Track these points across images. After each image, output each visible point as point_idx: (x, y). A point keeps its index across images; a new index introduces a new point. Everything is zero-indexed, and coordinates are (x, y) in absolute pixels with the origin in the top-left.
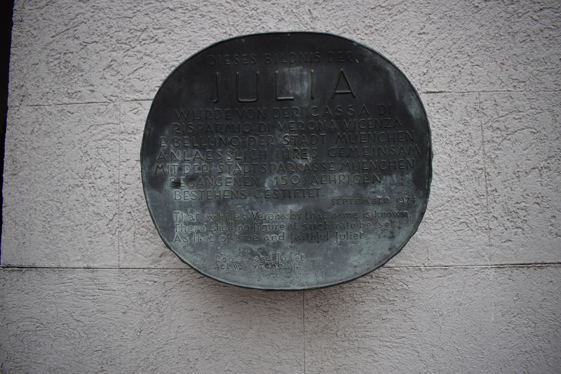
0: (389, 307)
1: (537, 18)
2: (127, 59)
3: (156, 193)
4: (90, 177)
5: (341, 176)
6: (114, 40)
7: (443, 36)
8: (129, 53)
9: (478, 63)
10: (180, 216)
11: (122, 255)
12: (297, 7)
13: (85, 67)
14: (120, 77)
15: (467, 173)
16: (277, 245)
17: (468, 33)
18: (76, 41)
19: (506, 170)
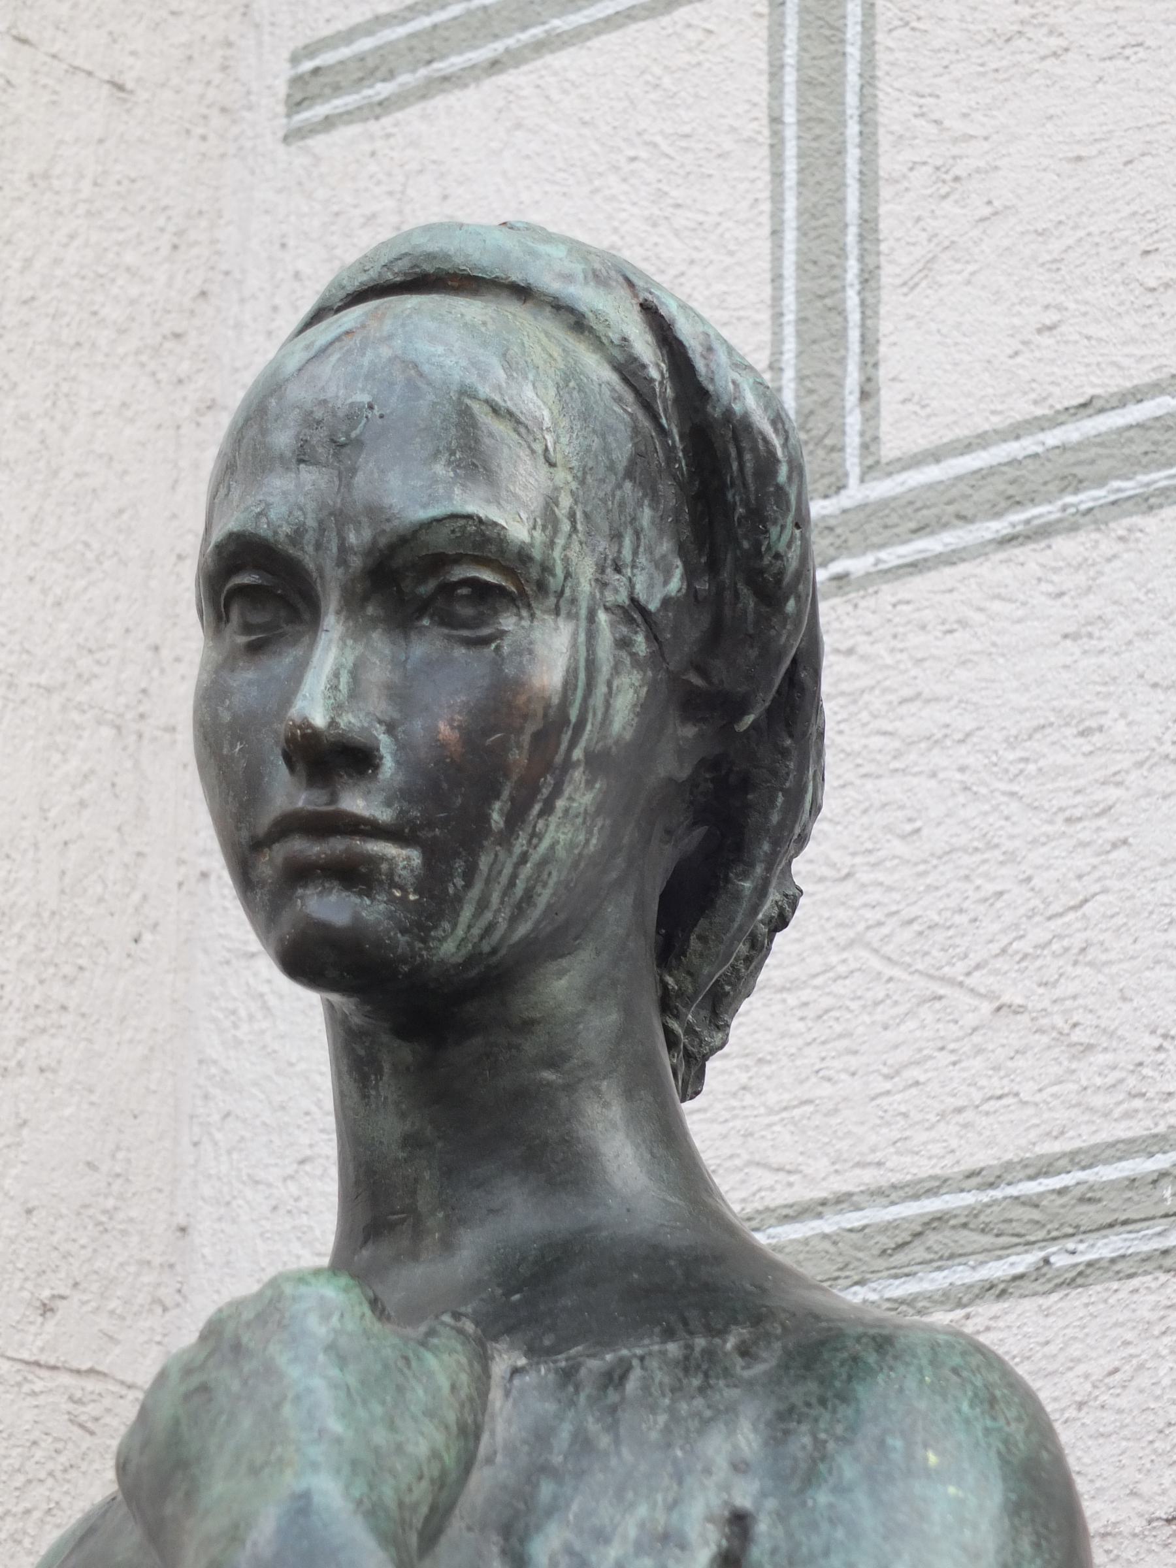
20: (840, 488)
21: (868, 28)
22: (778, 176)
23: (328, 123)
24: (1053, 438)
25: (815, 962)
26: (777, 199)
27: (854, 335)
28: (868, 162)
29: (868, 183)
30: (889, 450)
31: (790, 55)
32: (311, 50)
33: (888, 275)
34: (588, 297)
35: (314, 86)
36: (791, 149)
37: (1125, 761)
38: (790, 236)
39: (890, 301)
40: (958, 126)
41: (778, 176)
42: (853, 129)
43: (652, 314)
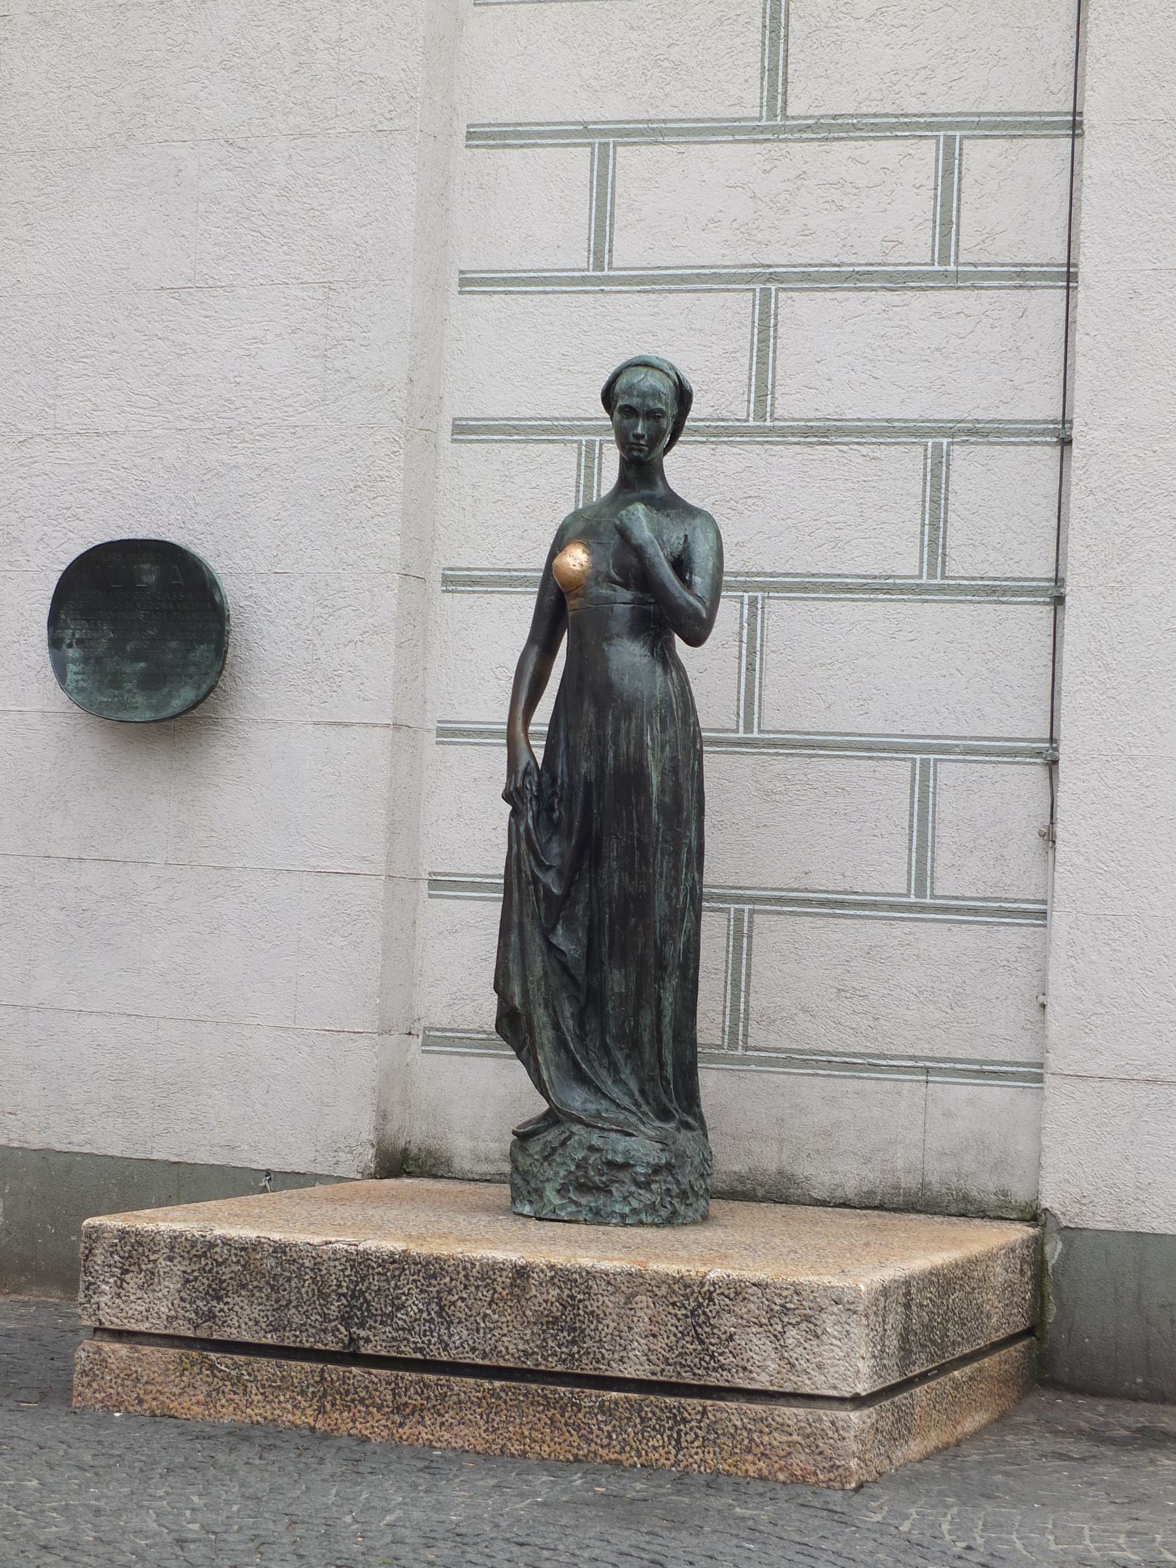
0: (232, 751)
1: (370, 506)
2: (55, 534)
3: (55, 650)
4: (24, 635)
5: (174, 645)
6: (45, 516)
7: (293, 522)
8: (57, 528)
9: (318, 547)
10: (72, 668)
11: (46, 701)
12: (185, 493)
13: (23, 538)
14: (50, 550)
15: (300, 643)
16: (129, 691)
17: (313, 520)
18: (16, 515)
19: (329, 642)
20: (603, 270)
21: (614, 168)
22: (591, 196)
23: (477, 146)
24: (651, 272)
25: (593, 370)
26: (591, 201)
27: (608, 237)
28: (613, 199)
31: (596, 167)
32: (473, 126)
33: (616, 226)
34: (670, 372)
35: (473, 135)
36: (595, 190)
37: (661, 343)
38: (594, 210)
40: (635, 198)
41: (591, 196)
42: (609, 190)
43: (678, 376)
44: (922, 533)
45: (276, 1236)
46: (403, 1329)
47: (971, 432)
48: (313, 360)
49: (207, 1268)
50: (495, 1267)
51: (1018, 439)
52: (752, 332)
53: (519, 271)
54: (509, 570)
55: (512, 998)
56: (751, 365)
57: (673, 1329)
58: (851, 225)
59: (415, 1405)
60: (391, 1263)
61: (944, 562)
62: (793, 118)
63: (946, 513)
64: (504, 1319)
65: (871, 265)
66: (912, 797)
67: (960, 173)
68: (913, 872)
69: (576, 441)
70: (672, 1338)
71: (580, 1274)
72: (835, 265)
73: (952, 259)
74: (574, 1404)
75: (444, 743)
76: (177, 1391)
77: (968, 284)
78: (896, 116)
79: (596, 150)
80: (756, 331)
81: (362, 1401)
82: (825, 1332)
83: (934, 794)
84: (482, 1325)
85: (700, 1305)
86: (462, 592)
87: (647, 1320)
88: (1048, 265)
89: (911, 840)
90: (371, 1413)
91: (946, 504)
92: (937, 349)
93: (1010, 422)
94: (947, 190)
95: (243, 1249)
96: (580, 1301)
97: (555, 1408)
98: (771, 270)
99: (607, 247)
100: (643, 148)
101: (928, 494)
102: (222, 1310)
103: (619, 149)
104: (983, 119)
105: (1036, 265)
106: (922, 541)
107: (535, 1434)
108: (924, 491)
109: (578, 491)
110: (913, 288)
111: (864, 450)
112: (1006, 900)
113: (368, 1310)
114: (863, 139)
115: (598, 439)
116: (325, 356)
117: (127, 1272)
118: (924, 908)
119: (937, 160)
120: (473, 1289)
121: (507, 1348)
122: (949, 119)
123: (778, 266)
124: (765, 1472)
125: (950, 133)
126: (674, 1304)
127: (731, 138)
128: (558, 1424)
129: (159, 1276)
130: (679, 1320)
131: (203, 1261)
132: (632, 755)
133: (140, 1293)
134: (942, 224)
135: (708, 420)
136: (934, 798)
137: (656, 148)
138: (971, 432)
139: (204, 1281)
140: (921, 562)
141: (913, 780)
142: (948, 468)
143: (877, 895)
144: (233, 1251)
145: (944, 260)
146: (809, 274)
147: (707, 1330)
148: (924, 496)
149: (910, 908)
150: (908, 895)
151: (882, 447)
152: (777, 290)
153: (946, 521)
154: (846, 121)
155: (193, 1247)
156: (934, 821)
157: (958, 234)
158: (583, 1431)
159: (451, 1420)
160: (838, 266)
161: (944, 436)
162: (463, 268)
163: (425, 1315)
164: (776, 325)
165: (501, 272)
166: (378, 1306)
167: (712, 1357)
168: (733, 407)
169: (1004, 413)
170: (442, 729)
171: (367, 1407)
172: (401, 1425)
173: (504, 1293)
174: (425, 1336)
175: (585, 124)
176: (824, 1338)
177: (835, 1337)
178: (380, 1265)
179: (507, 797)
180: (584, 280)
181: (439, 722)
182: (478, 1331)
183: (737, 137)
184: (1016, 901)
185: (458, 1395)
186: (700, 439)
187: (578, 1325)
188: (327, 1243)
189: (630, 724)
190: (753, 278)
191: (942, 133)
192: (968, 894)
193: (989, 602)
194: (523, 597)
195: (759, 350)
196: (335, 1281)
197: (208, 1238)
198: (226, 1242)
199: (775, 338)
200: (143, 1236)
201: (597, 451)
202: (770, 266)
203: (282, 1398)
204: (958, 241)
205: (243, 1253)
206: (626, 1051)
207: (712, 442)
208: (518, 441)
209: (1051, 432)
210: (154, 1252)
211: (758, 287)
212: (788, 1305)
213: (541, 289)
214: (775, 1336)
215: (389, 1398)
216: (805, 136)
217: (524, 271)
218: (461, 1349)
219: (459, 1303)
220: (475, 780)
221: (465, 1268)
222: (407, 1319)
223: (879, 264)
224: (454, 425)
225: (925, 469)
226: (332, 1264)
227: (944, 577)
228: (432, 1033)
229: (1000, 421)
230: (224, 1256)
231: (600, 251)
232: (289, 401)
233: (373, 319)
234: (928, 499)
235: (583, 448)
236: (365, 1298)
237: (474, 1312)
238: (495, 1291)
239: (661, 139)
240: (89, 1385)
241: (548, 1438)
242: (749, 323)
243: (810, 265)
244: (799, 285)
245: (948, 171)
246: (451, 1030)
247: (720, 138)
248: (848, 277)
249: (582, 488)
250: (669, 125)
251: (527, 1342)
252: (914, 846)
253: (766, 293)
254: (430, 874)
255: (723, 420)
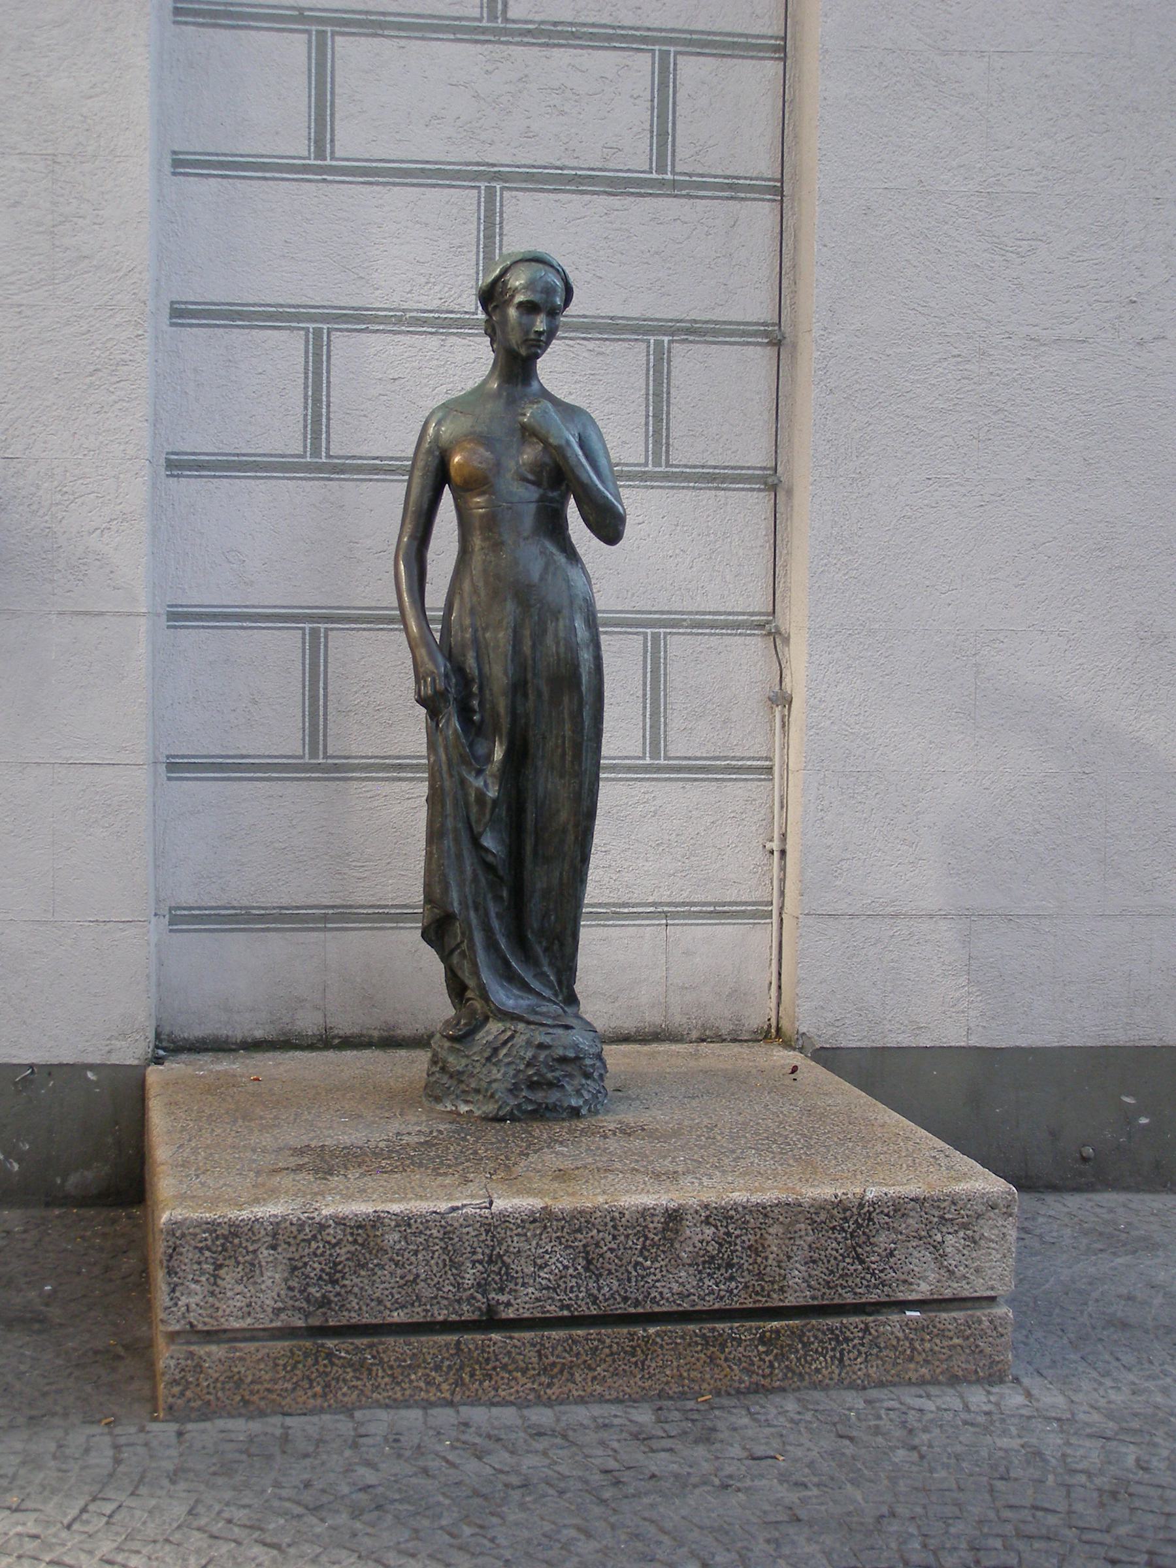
17: (48, 403)
23: (186, 23)
24: (374, 165)
28: (333, 88)
29: (333, 93)
30: (337, 155)
33: (337, 116)
39: (337, 122)
41: (310, 83)
42: (329, 79)
44: (647, 424)
45: (395, 1208)
46: (548, 1288)
47: (689, 331)
48: (37, 237)
49: (319, 1252)
50: (645, 1213)
51: (732, 339)
52: (479, 229)
53: (236, 155)
54: (238, 455)
55: (452, 904)
56: (478, 260)
57: (834, 1253)
58: (573, 130)
59: (564, 1364)
60: (531, 1222)
61: (667, 452)
62: (514, 21)
63: (668, 406)
64: (658, 1265)
65: (593, 169)
66: (645, 667)
67: (675, 87)
68: (648, 737)
69: (303, 328)
70: (833, 1261)
71: (736, 1210)
72: (557, 168)
73: (669, 169)
74: (734, 1339)
75: (175, 627)
76: (289, 1386)
77: (684, 192)
78: (613, 28)
79: (314, 38)
80: (482, 227)
81: (504, 1367)
82: (982, 1236)
83: (665, 664)
84: (634, 1273)
85: (859, 1226)
86: (188, 476)
87: (806, 1247)
88: (757, 179)
89: (645, 708)
90: (515, 1379)
91: (668, 398)
92: (657, 253)
93: (725, 323)
94: (663, 102)
95: (360, 1227)
96: (737, 1237)
97: (714, 1346)
98: (496, 169)
99: (328, 136)
100: (363, 39)
101: (651, 388)
102: (338, 1294)
103: (338, 39)
104: (694, 37)
105: (746, 178)
106: (647, 431)
107: (693, 1374)
108: (647, 385)
109: (306, 378)
110: (632, 194)
111: (591, 345)
112: (733, 758)
113: (507, 1274)
114: (582, 47)
115: (325, 327)
116: (52, 232)
117: (220, 1266)
118: (659, 769)
119: (653, 73)
120: (622, 1238)
121: (661, 1293)
122: (663, 34)
123: (502, 165)
124: (928, 1377)
125: (664, 48)
126: (834, 1228)
127: (452, 37)
128: (718, 1361)
129: (261, 1266)
130: (839, 1243)
131: (314, 1245)
132: (562, 656)
133: (240, 1288)
134: (658, 135)
135: (437, 312)
136: (665, 668)
137: (376, 40)
138: (689, 331)
139: (316, 1265)
140: (647, 451)
141: (645, 652)
142: (669, 364)
143: (614, 758)
144: (348, 1230)
145: (661, 169)
146: (533, 174)
147: (868, 1249)
148: (647, 389)
149: (646, 769)
150: (643, 758)
151: (607, 343)
152: (502, 189)
153: (668, 413)
154: (566, 29)
155: (299, 1231)
156: (665, 690)
157: (673, 145)
158: (744, 1364)
159: (603, 1374)
160: (561, 169)
161: (664, 335)
162: (176, 149)
163: (571, 1271)
164: (501, 223)
165: (217, 155)
166: (519, 1268)
167: (873, 1274)
168: (460, 301)
169: (718, 315)
170: (173, 613)
171: (510, 1372)
172: (550, 1385)
173: (656, 1238)
174: (572, 1292)
175: (301, 9)
176: (982, 1242)
177: (992, 1241)
178: (519, 1226)
179: (422, 701)
180: (306, 169)
181: (169, 606)
182: (629, 1280)
183: (459, 36)
184: (742, 759)
185: (610, 1347)
186: (430, 330)
187: (735, 1260)
188: (454, 1209)
189: (557, 625)
190: (477, 176)
191: (657, 47)
192: (698, 754)
193: (710, 489)
194: (253, 482)
195: (485, 246)
196: (469, 1249)
197: (317, 1220)
198: (340, 1222)
199: (501, 235)
200: (238, 1226)
201: (325, 338)
202: (494, 165)
203: (413, 1377)
204: (674, 151)
205: (360, 1231)
206: (544, 944)
207: (442, 333)
208: (242, 327)
209: (766, 334)
210: (254, 1242)
211: (483, 185)
212: (947, 1216)
213: (259, 174)
214: (934, 1247)
215: (535, 1360)
216: (525, 40)
217: (242, 156)
218: (611, 1301)
219: (609, 1254)
220: (211, 663)
221: (613, 1219)
222: (552, 1278)
223: (601, 170)
224: (172, 309)
225: (648, 364)
226: (465, 1230)
227: (668, 465)
228: (178, 912)
229: (716, 322)
230: (338, 1237)
231: (321, 138)
232: (13, 279)
233: (106, 197)
234: (651, 392)
235: (311, 335)
236: (503, 1262)
237: (624, 1261)
238: (646, 1238)
239: (380, 32)
240: (182, 1394)
241: (708, 1376)
242: (475, 218)
243: (534, 167)
244: (524, 185)
245: (664, 85)
246: (199, 908)
247: (441, 36)
248: (572, 179)
249: (310, 375)
250: (388, 19)
251: (682, 1284)
252: (648, 713)
253: (491, 191)
254: (168, 757)
255: (452, 312)
